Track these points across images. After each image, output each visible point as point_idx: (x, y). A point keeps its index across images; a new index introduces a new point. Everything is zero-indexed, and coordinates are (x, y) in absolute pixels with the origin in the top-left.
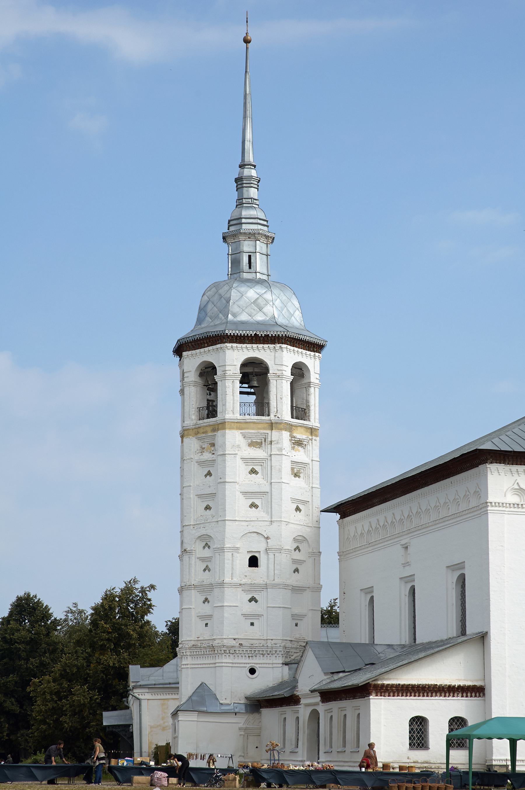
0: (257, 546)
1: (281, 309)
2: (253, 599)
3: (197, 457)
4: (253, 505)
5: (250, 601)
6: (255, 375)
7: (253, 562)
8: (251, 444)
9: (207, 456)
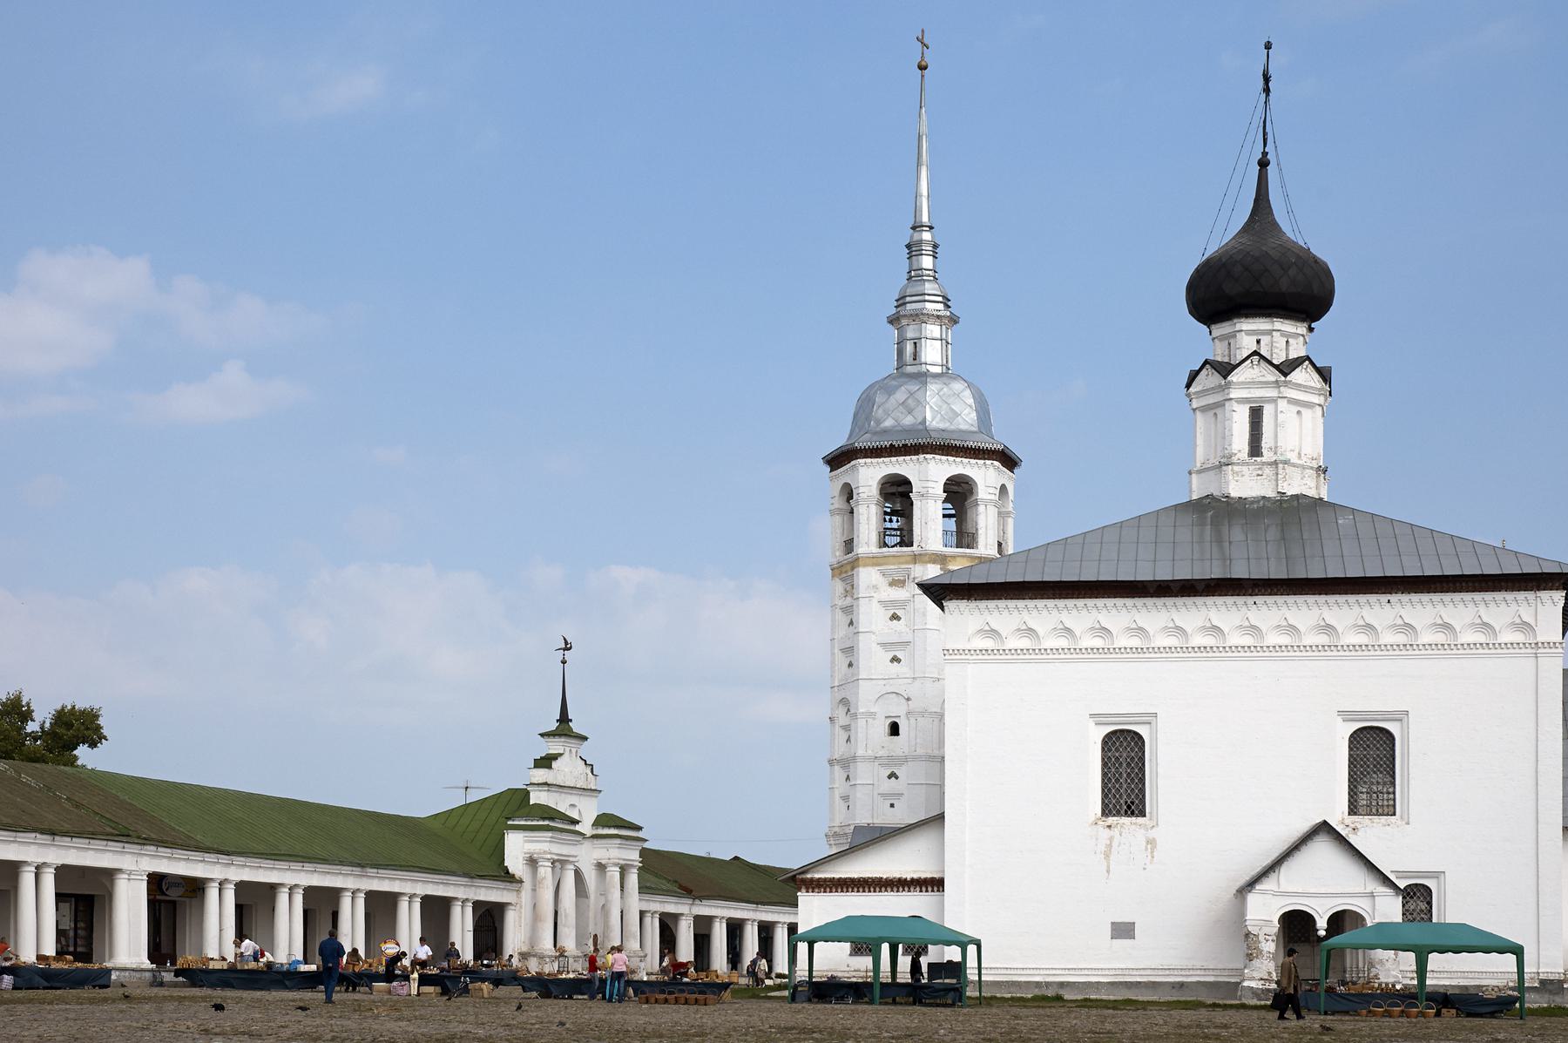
0: (898, 710)
1: (947, 408)
2: (893, 775)
3: (840, 603)
4: (895, 659)
5: (889, 777)
6: (897, 493)
7: (894, 729)
8: (891, 584)
9: (849, 601)
